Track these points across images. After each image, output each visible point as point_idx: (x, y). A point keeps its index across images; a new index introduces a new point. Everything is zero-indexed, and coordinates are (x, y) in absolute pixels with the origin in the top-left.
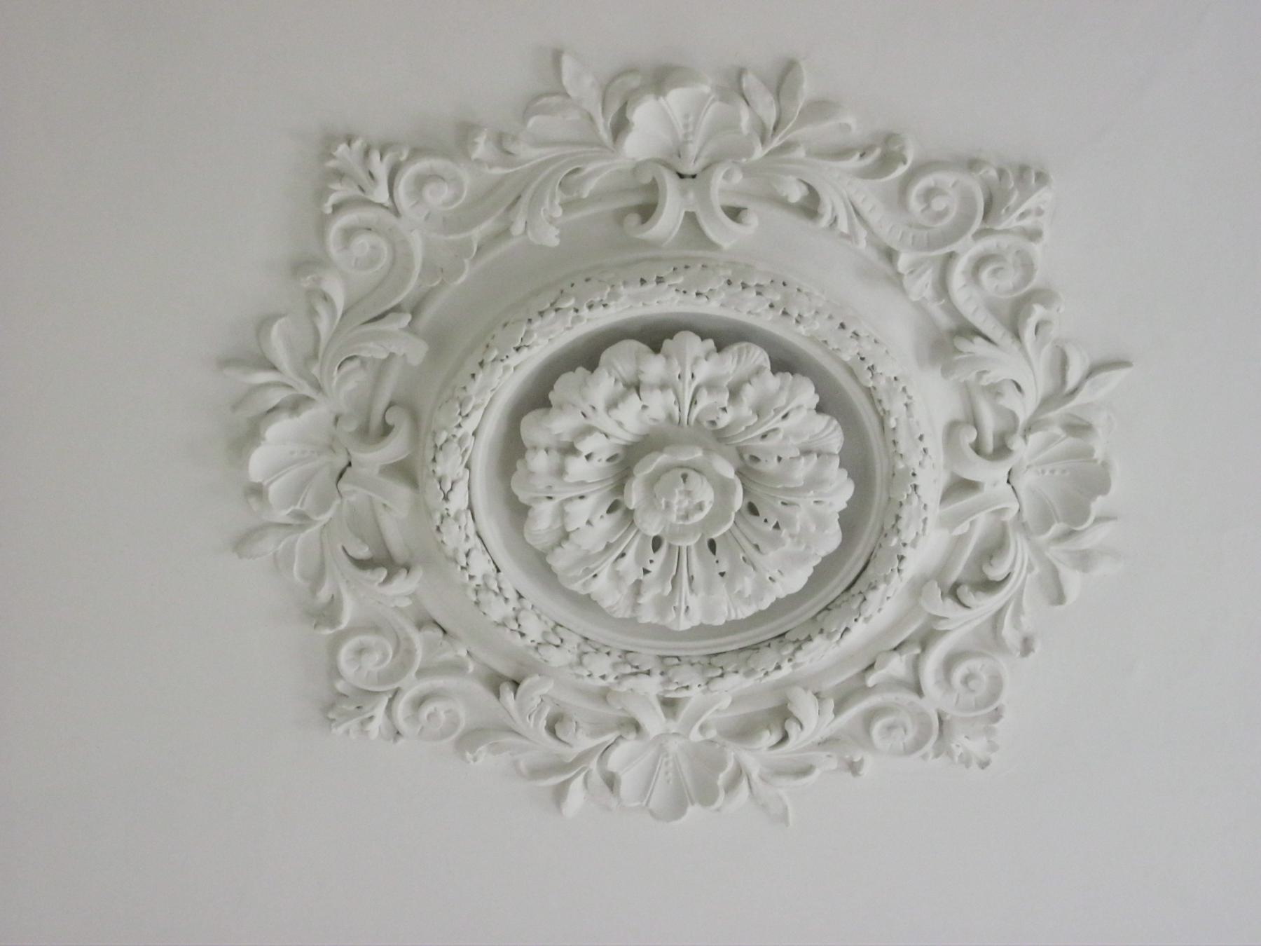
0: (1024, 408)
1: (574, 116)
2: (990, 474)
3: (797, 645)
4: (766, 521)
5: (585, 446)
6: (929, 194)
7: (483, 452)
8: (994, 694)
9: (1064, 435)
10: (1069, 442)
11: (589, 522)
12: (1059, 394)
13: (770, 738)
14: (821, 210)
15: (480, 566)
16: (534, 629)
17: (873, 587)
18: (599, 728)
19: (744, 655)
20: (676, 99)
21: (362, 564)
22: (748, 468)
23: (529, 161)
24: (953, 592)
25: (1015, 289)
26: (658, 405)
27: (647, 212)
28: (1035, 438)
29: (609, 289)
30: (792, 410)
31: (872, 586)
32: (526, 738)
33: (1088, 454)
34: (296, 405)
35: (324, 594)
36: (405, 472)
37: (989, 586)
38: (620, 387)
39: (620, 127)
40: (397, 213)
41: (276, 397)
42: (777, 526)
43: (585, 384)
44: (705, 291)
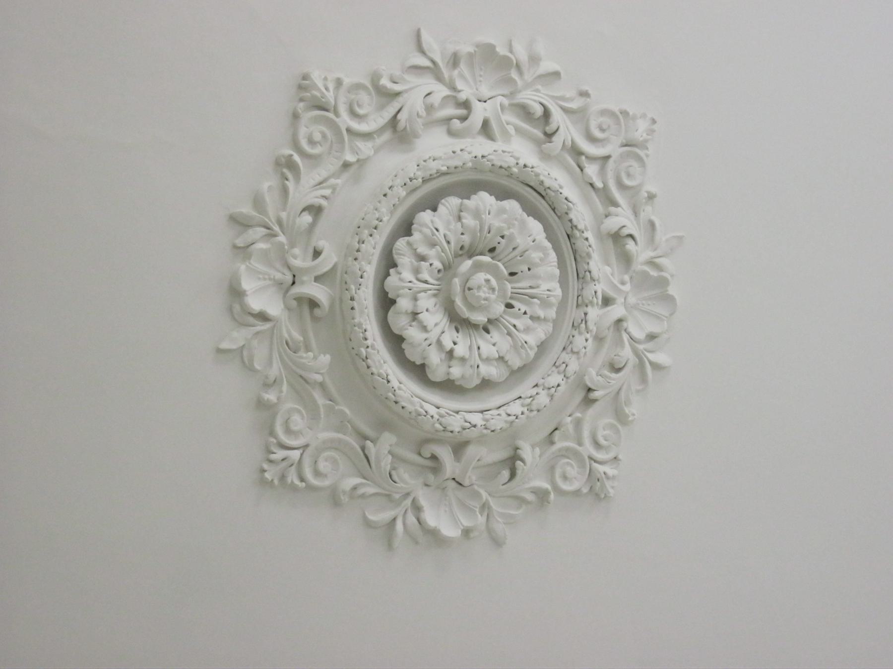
0: (442, 91)
1: (255, 343)
2: (480, 112)
3: (574, 228)
4: (499, 243)
5: (448, 345)
6: (311, 142)
7: (449, 403)
9: (459, 69)
10: (463, 66)
11: (494, 345)
12: (434, 71)
13: (630, 245)
14: (317, 205)
15: (516, 408)
16: (555, 379)
17: (542, 183)
18: (619, 343)
19: (578, 257)
20: (247, 284)
21: (513, 475)
22: (466, 251)
23: (280, 369)
24: (549, 136)
25: (370, 94)
26: (426, 302)
27: (313, 304)
28: (460, 85)
29: (356, 328)
30: (433, 226)
31: (541, 183)
32: (623, 385)
33: (471, 56)
34: (417, 508)
35: (530, 497)
36: (459, 448)
37: (547, 114)
38: (414, 323)
39: (263, 317)
40: (307, 446)
41: (411, 519)
42: (502, 237)
43: (411, 344)
44: (360, 273)
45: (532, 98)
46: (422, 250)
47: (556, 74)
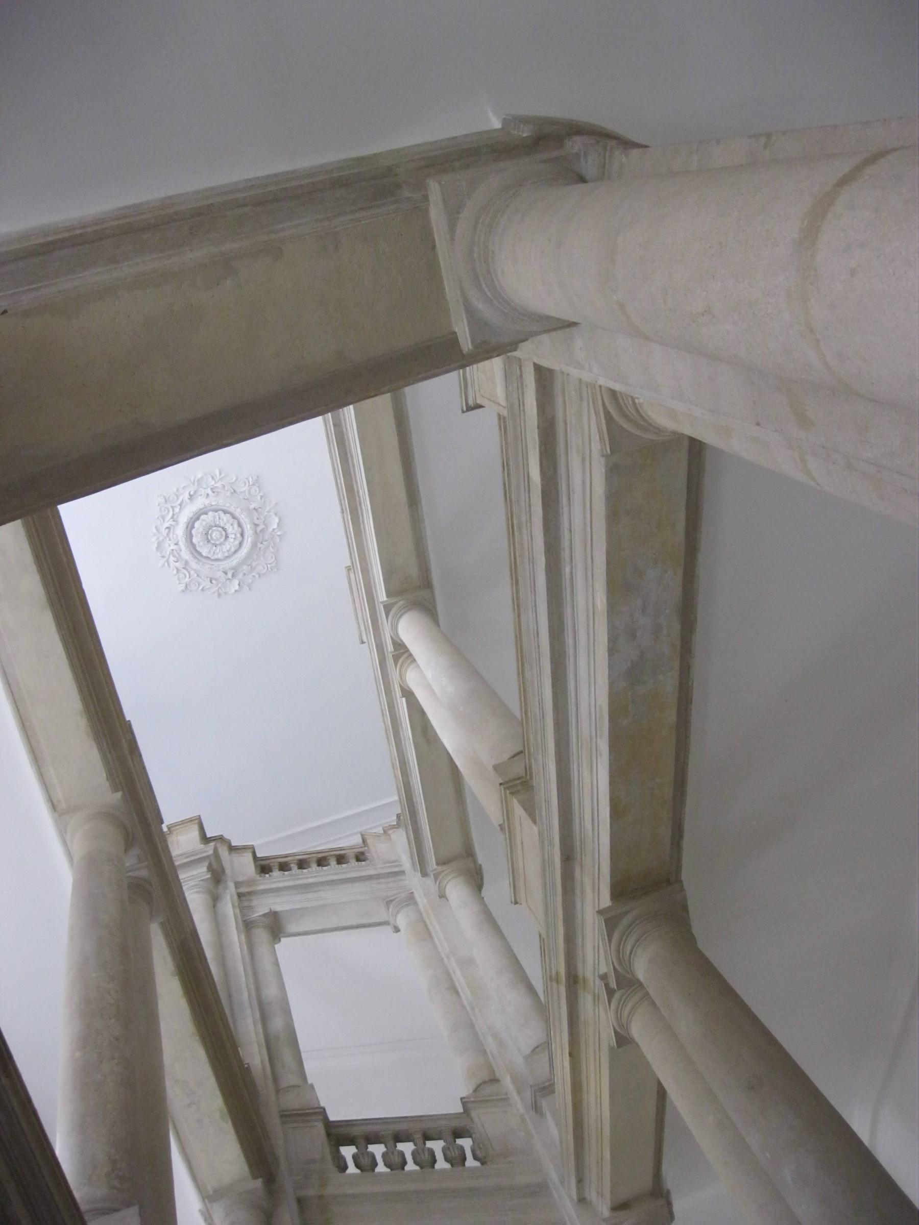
0: (172, 559)
2: (173, 547)
8: (160, 509)
10: (163, 554)
12: (167, 561)
13: (192, 493)
15: (243, 516)
20: (233, 591)
24: (171, 525)
27: (233, 573)
28: (168, 553)
33: (161, 553)
34: (274, 529)
37: (167, 528)
39: (239, 585)
45: (165, 533)
46: (212, 553)
47: (156, 527)
